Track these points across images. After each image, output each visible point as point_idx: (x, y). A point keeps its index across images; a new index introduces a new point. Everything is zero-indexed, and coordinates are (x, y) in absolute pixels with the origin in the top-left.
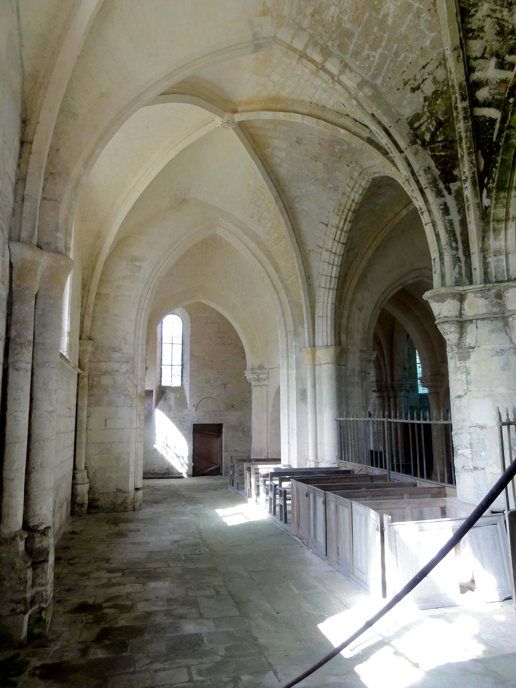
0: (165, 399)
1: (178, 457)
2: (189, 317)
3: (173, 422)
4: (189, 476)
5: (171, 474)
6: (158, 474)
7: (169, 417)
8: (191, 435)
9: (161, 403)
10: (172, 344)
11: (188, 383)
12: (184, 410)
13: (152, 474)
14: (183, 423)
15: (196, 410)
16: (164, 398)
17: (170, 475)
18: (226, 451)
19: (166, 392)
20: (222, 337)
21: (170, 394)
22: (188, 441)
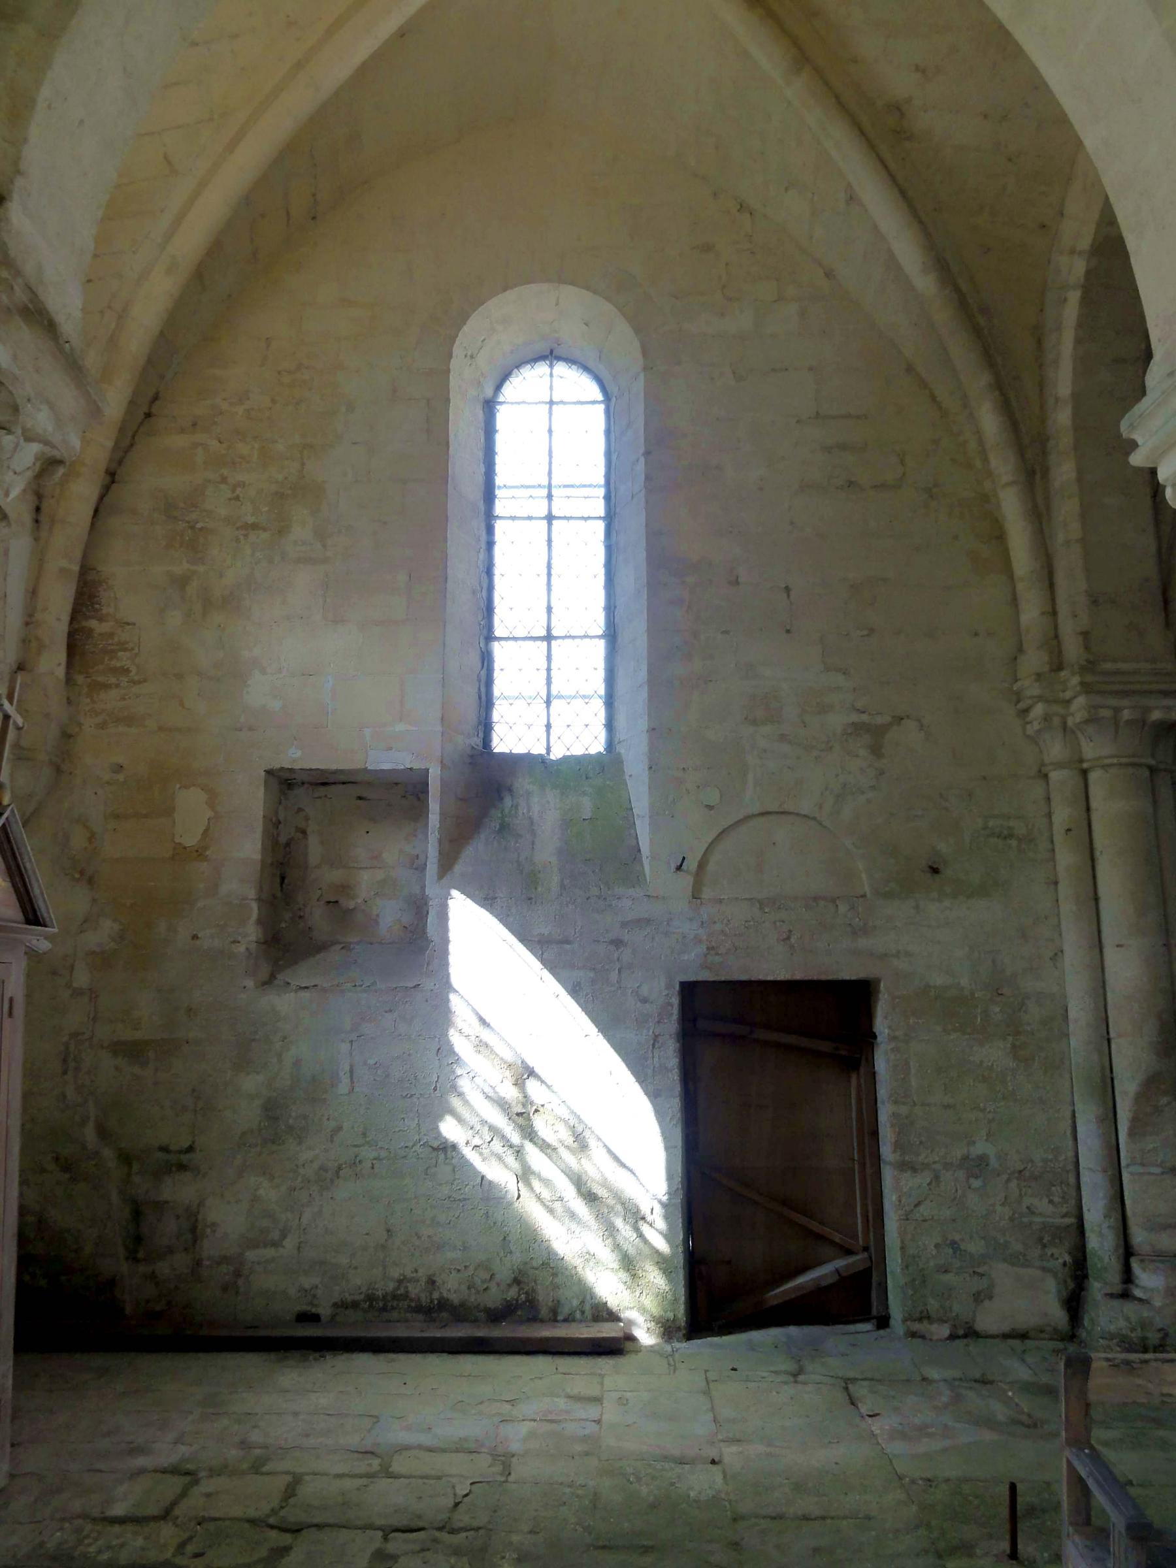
0: (504, 828)
1: (590, 1198)
2: (637, 344)
3: (551, 966)
4: (668, 1330)
5: (544, 1312)
6: (459, 1312)
7: (524, 938)
8: (669, 1056)
9: (477, 849)
10: (550, 518)
11: (643, 724)
12: (619, 890)
13: (419, 1309)
14: (614, 976)
15: (696, 895)
16: (496, 825)
17: (534, 1319)
18: (903, 1166)
19: (510, 790)
20: (843, 447)
21: (535, 799)
22: (654, 1095)
